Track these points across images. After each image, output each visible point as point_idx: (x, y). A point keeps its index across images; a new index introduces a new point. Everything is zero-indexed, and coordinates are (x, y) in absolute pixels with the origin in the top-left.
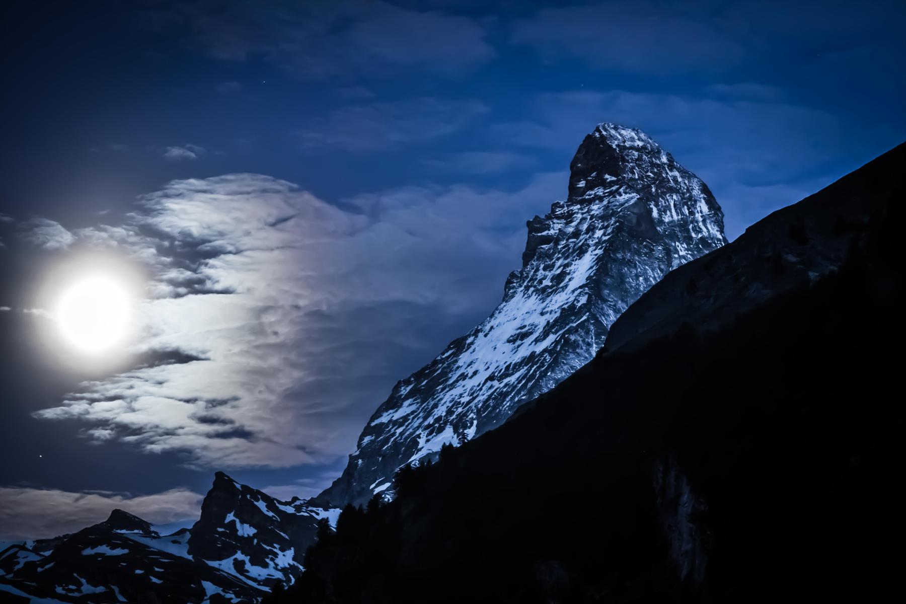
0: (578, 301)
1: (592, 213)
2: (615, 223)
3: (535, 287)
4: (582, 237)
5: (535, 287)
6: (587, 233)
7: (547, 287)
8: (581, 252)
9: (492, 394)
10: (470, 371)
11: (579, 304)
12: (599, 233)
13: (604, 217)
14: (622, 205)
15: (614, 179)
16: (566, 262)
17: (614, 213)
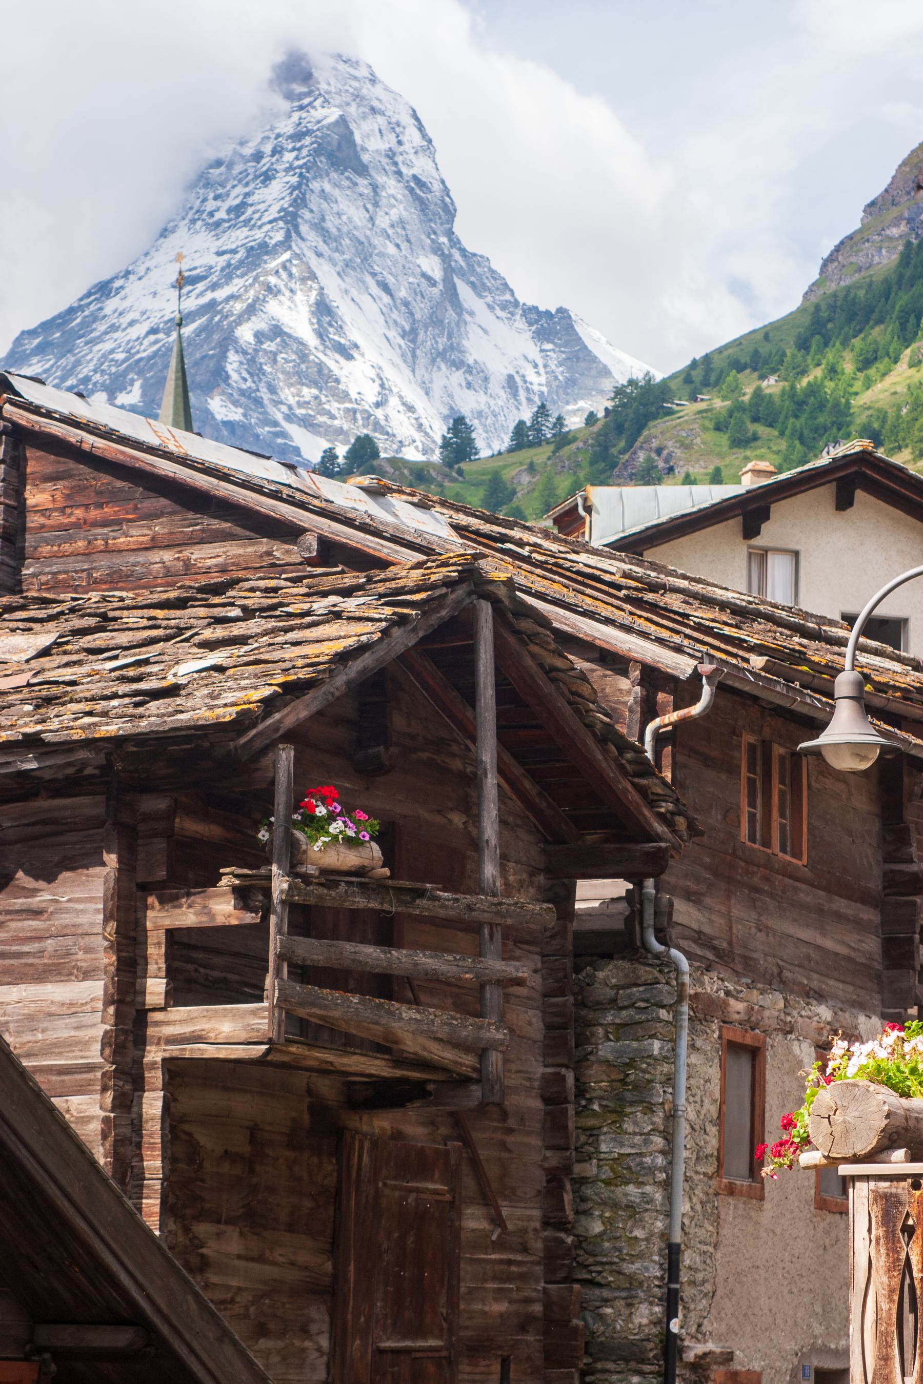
0: (271, 238)
1: (277, 131)
2: (312, 143)
3: (204, 220)
4: (264, 161)
5: (204, 220)
6: (274, 152)
7: (224, 221)
8: (267, 177)
9: (159, 350)
10: (124, 321)
11: (273, 242)
12: (289, 157)
13: (298, 136)
14: (319, 122)
15: (304, 89)
16: (247, 190)
17: (308, 132)
